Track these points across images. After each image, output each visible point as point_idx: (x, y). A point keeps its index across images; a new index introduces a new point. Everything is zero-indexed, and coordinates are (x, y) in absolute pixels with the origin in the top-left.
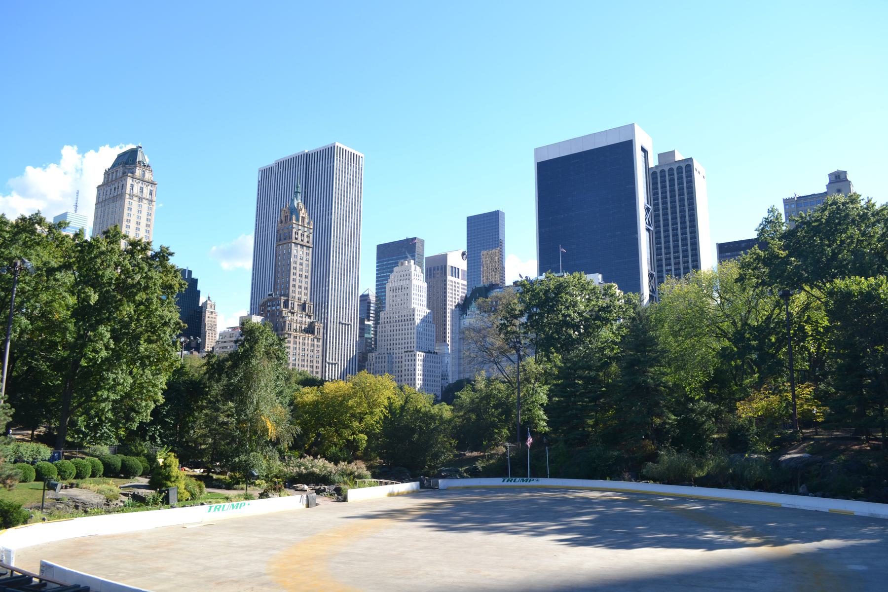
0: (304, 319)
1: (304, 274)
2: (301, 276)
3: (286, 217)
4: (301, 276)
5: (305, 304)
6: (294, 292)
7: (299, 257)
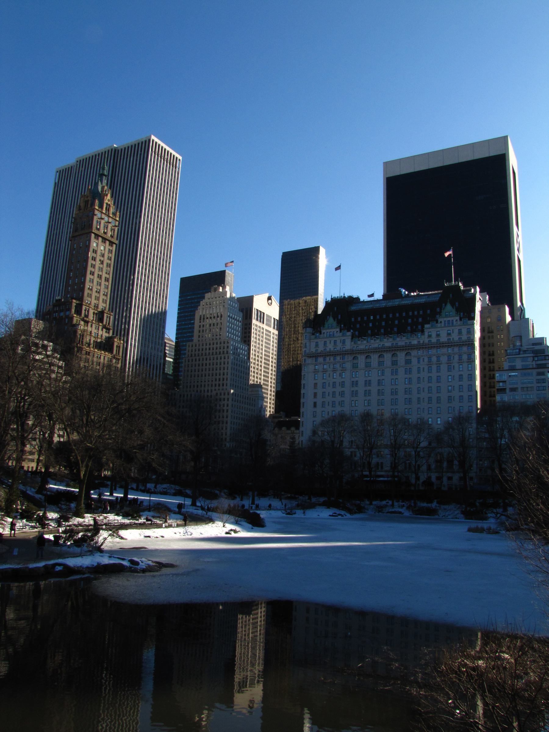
0: (100, 333)
1: (104, 275)
2: (100, 277)
3: (87, 202)
4: (100, 277)
5: (102, 313)
6: (90, 296)
7: (99, 253)
